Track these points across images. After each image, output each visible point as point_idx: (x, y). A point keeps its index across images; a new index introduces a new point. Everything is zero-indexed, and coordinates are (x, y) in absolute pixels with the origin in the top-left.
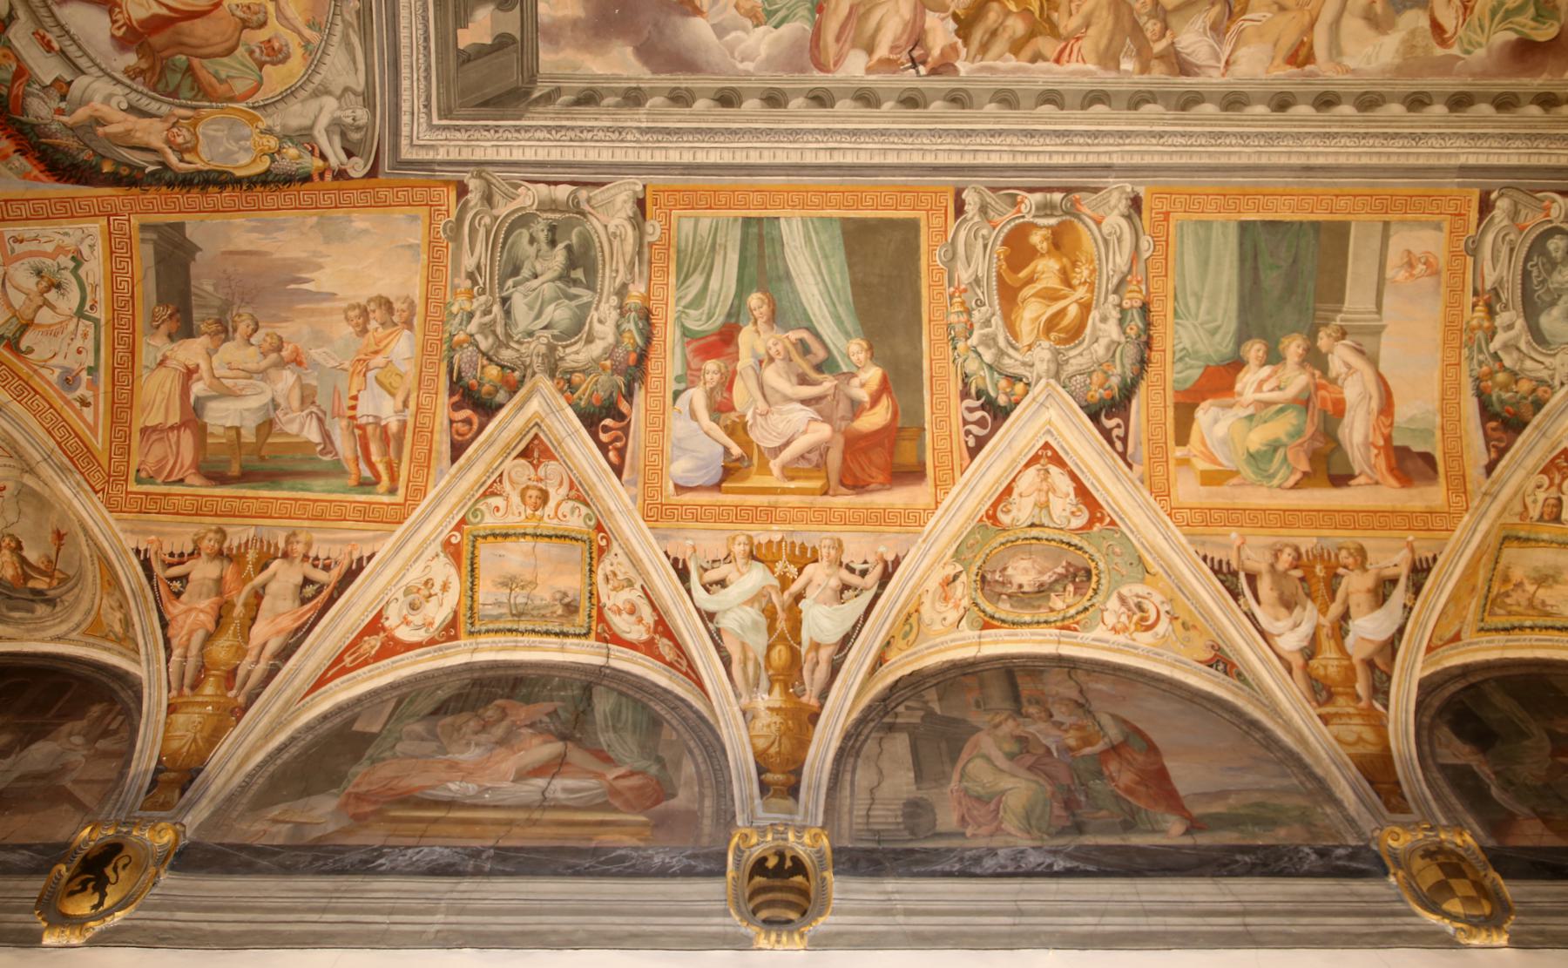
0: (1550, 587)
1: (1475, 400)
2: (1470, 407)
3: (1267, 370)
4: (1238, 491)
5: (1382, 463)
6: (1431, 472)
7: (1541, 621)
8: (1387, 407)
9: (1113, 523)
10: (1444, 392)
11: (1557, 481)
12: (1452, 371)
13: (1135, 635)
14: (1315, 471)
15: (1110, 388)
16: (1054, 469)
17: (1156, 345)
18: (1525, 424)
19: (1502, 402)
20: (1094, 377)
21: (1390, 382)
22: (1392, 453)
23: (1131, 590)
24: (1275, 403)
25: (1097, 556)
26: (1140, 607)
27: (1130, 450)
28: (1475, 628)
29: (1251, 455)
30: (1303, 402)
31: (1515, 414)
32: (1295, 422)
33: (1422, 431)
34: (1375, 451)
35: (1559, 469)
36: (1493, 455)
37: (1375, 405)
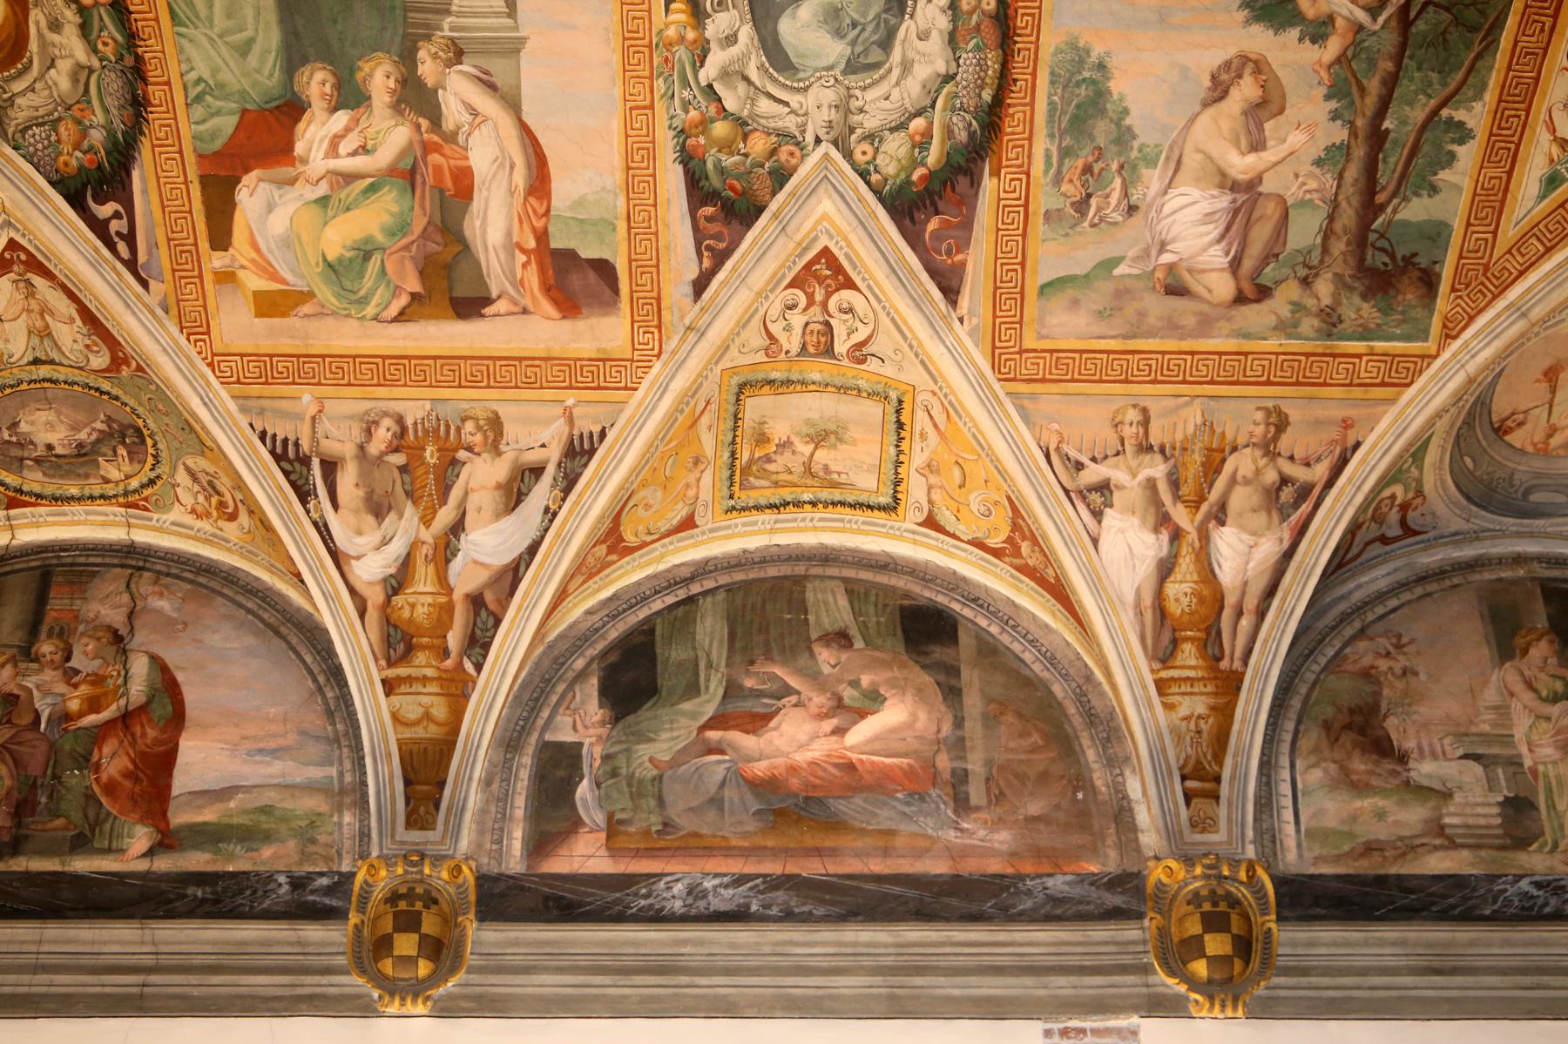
0: (834, 447)
1: (679, 169)
2: (672, 180)
3: (342, 118)
4: (314, 325)
5: (533, 278)
6: (608, 292)
7: (825, 494)
8: (539, 183)
9: (139, 368)
10: (628, 155)
11: (819, 297)
12: (640, 120)
13: (221, 523)
14: (429, 290)
15: (91, 149)
16: (38, 281)
17: (152, 76)
18: (760, 210)
19: (722, 171)
20: (62, 129)
21: (542, 141)
22: (548, 260)
23: (199, 463)
24: (361, 176)
25: (140, 410)
26: (210, 483)
27: (142, 257)
28: (719, 509)
29: (330, 265)
30: (407, 174)
31: (744, 193)
32: (395, 209)
33: (595, 223)
34: (523, 258)
35: (821, 280)
36: (706, 263)
37: (520, 178)
